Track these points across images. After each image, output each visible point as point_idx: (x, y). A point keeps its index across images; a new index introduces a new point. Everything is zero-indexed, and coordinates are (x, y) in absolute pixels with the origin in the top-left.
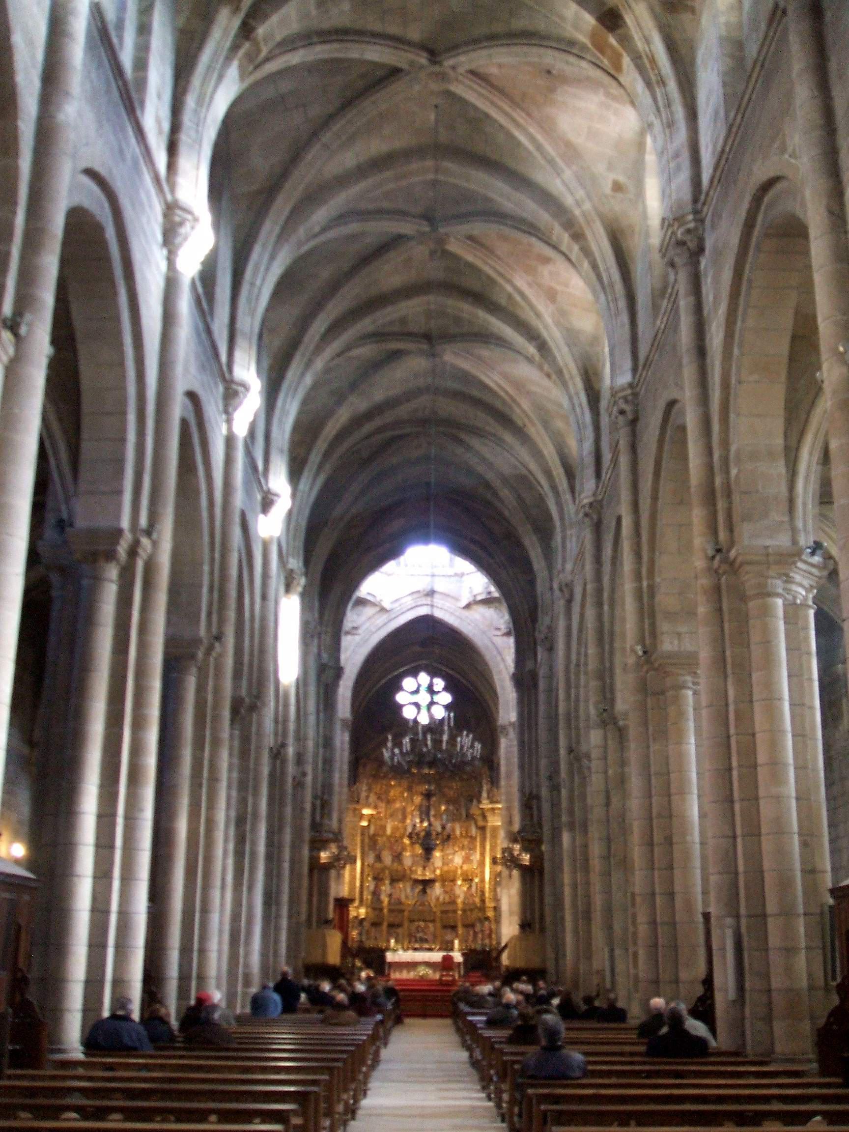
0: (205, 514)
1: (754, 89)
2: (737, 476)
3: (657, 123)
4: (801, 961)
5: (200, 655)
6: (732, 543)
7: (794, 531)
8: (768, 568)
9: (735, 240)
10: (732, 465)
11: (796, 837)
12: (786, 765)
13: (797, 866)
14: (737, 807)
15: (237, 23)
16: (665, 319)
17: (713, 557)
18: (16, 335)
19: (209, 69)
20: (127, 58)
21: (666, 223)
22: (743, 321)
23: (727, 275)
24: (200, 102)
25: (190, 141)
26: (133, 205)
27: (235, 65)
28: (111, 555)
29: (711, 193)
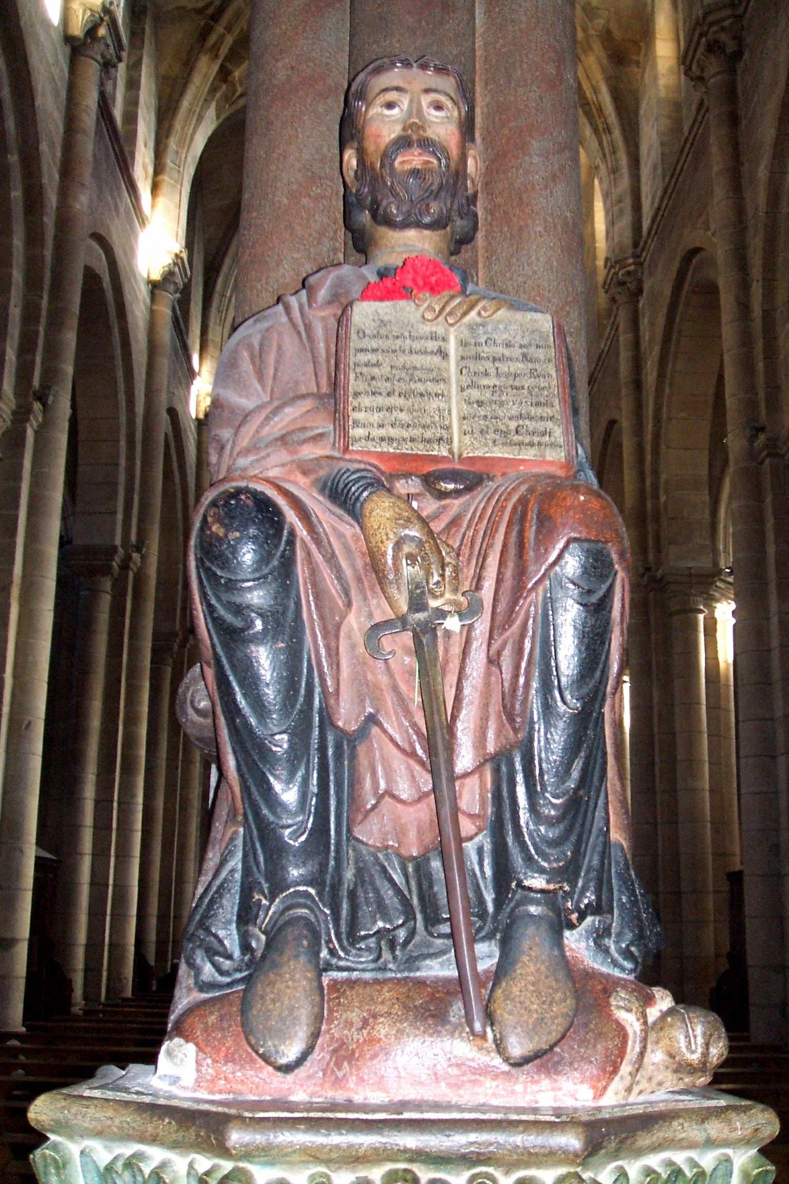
0: (180, 516)
1: (685, 161)
2: (665, 503)
3: (603, 167)
4: (709, 934)
5: (176, 647)
6: (659, 563)
7: (715, 552)
8: (691, 587)
9: (668, 292)
10: (661, 492)
11: (709, 825)
12: (701, 761)
13: (710, 850)
14: (659, 797)
15: (216, 68)
16: (609, 343)
17: (643, 575)
18: (44, 405)
19: (190, 111)
20: (118, 113)
21: (609, 264)
22: (674, 363)
23: (661, 321)
24: (181, 144)
25: (172, 182)
26: (125, 253)
27: (213, 105)
28: (106, 570)
29: (649, 242)
